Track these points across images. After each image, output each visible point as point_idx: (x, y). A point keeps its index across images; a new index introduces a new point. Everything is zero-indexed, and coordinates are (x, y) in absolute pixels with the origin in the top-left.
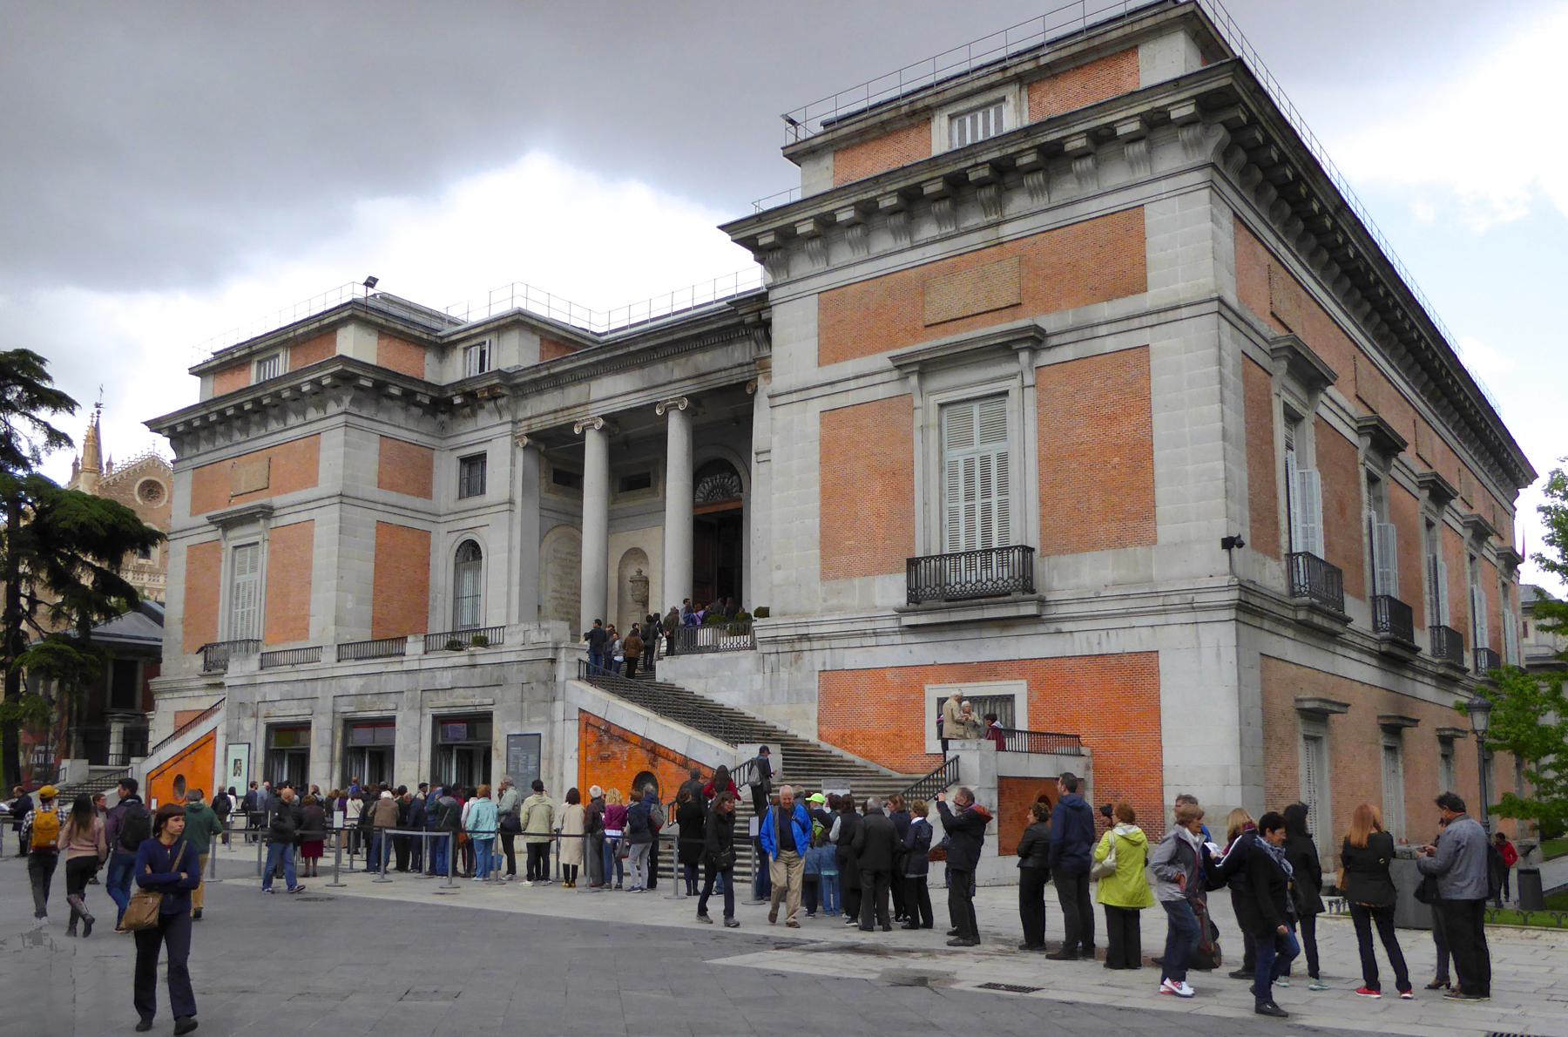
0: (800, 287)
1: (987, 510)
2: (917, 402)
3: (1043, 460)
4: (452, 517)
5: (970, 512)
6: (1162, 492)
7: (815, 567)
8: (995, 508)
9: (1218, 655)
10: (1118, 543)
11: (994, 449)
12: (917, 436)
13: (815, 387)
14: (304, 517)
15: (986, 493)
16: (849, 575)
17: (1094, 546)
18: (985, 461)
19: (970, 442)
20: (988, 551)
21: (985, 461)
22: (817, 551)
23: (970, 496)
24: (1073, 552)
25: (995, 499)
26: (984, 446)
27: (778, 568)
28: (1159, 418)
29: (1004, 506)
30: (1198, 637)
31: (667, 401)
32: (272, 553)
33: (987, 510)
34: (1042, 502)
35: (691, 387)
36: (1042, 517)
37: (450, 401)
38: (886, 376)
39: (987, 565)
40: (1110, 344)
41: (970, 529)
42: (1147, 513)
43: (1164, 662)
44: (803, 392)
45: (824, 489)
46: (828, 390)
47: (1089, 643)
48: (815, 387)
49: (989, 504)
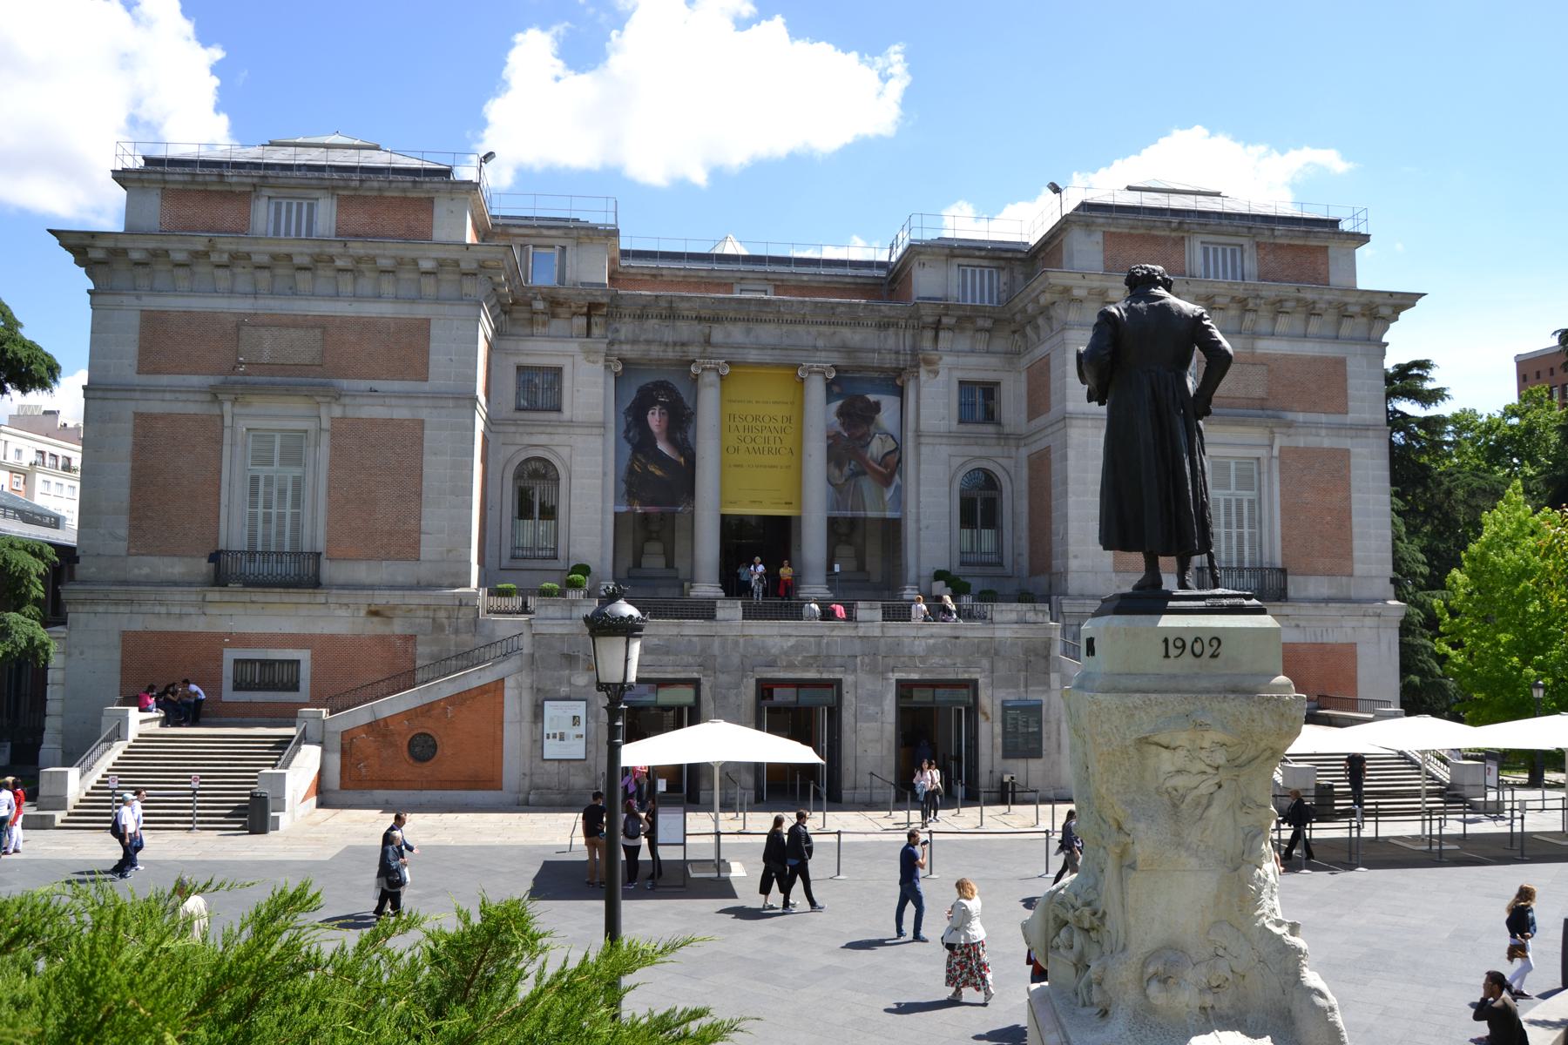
1: (1240, 537)
3: (1283, 510)
5: (1228, 536)
6: (1356, 543)
8: (1246, 536)
9: (1390, 648)
10: (1329, 573)
11: (1246, 495)
14: (402, 413)
15: (1240, 526)
17: (1315, 573)
18: (1239, 503)
19: (1227, 487)
23: (1228, 525)
24: (1302, 575)
25: (1246, 530)
26: (1238, 492)
27: (1076, 557)
28: (1355, 496)
30: (1379, 636)
31: (812, 367)
32: (335, 448)
33: (1240, 537)
34: (1283, 539)
35: (837, 359)
36: (1283, 548)
39: (1241, 576)
40: (1327, 443)
41: (1229, 548)
42: (1348, 554)
43: (1360, 650)
47: (1315, 634)
49: (1242, 533)
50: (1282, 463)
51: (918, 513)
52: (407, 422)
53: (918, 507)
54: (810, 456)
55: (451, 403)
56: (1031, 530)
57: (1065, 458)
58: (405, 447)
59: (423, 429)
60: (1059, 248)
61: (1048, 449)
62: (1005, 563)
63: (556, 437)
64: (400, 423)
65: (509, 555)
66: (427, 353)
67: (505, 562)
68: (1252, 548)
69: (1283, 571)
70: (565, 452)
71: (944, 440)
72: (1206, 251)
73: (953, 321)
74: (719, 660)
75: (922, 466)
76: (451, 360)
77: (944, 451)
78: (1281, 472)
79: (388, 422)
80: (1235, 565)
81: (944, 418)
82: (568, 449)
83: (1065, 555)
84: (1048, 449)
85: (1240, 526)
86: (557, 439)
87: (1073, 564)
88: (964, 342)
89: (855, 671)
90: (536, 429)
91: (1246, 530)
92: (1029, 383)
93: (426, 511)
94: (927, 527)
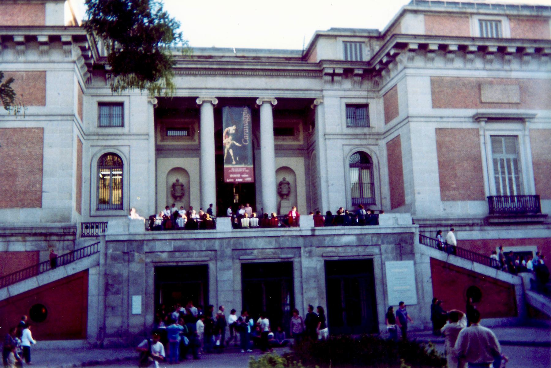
0: (422, 71)
1: (510, 179)
2: (481, 133)
4: (97, 137)
5: (504, 180)
7: (438, 194)
8: (514, 179)
11: (512, 157)
12: (482, 147)
13: (432, 117)
15: (510, 173)
16: (454, 199)
20: (512, 197)
21: (508, 161)
22: (438, 188)
23: (503, 173)
25: (513, 176)
27: (419, 193)
29: (517, 178)
33: (510, 179)
37: (103, 67)
38: (467, 120)
39: (513, 201)
41: (504, 186)
44: (427, 118)
45: (439, 162)
46: (439, 119)
48: (432, 117)
50: (531, 138)
51: (327, 178)
52: (33, 130)
53: (327, 174)
54: (265, 148)
55: (60, 118)
56: (391, 183)
57: (409, 138)
58: (33, 143)
59: (43, 133)
60: (400, 23)
61: (398, 137)
62: (377, 203)
63: (122, 141)
64: (30, 130)
65: (95, 208)
66: (44, 90)
67: (93, 213)
68: (518, 186)
69: (537, 198)
70: (125, 150)
71: (340, 137)
72: (481, 25)
73: (341, 71)
74: (219, 253)
75: (328, 151)
76: (59, 94)
77: (340, 142)
78: (531, 142)
79: (22, 129)
80: (509, 194)
81: (338, 125)
82: (127, 148)
83: (413, 193)
84: (398, 137)
85: (510, 173)
86: (121, 142)
87: (417, 197)
88: (347, 84)
89: (300, 256)
90: (109, 137)
91: (513, 176)
92: (385, 103)
93: (46, 180)
94: (332, 185)
